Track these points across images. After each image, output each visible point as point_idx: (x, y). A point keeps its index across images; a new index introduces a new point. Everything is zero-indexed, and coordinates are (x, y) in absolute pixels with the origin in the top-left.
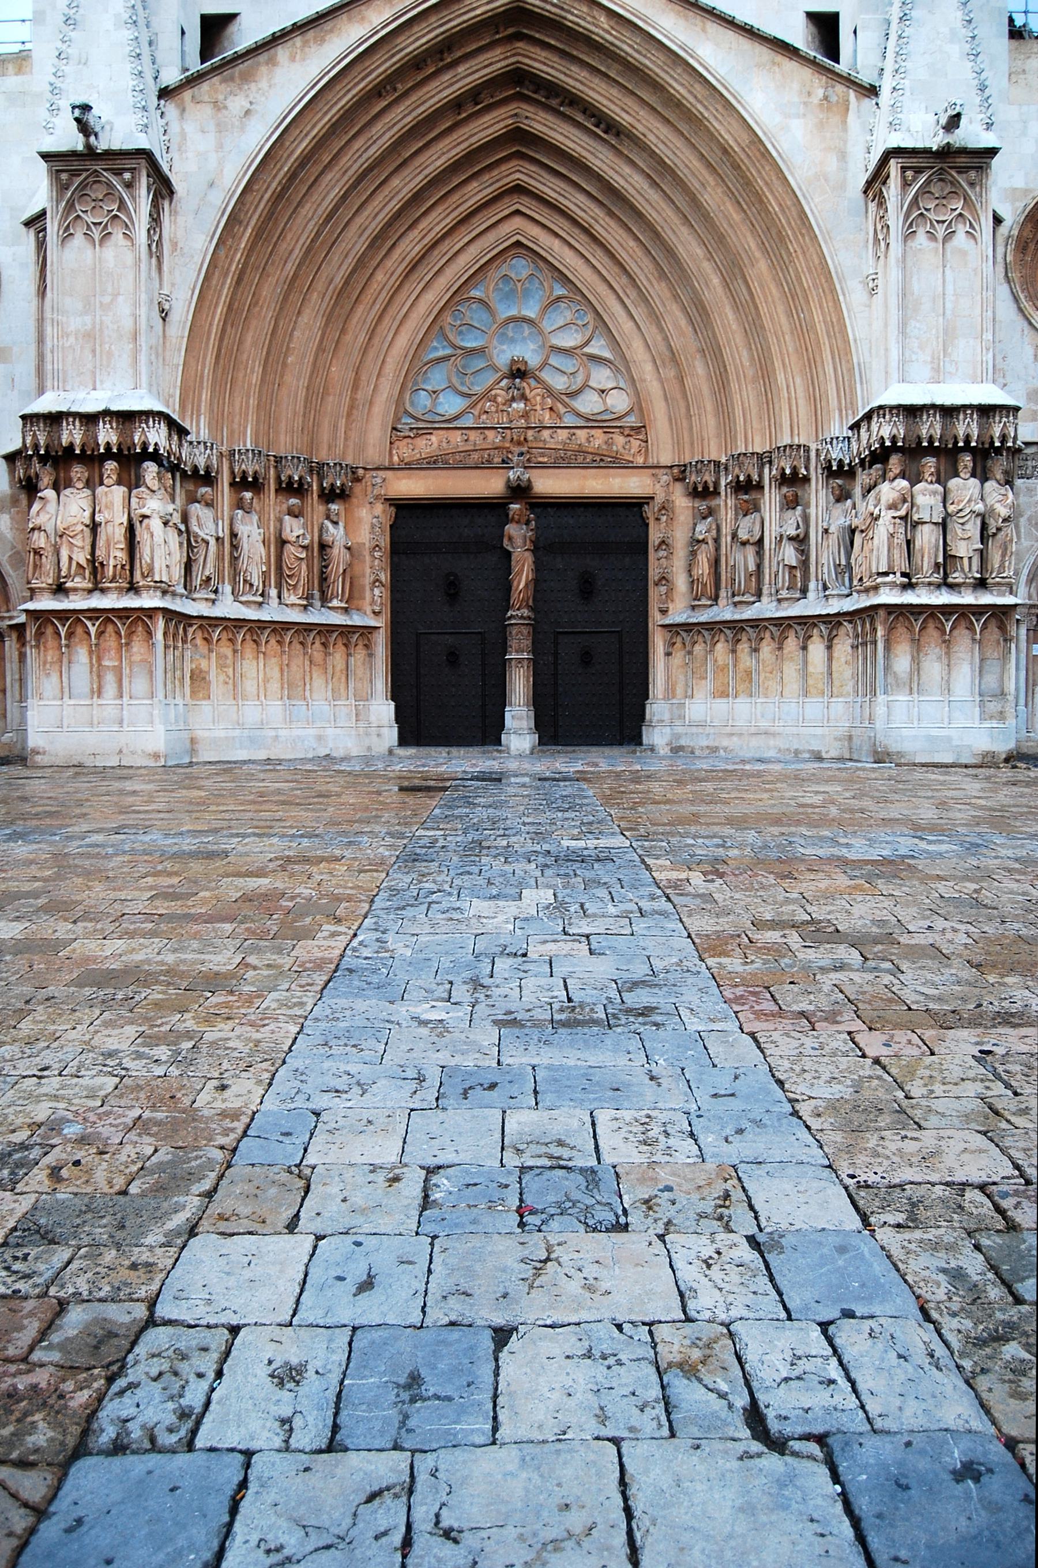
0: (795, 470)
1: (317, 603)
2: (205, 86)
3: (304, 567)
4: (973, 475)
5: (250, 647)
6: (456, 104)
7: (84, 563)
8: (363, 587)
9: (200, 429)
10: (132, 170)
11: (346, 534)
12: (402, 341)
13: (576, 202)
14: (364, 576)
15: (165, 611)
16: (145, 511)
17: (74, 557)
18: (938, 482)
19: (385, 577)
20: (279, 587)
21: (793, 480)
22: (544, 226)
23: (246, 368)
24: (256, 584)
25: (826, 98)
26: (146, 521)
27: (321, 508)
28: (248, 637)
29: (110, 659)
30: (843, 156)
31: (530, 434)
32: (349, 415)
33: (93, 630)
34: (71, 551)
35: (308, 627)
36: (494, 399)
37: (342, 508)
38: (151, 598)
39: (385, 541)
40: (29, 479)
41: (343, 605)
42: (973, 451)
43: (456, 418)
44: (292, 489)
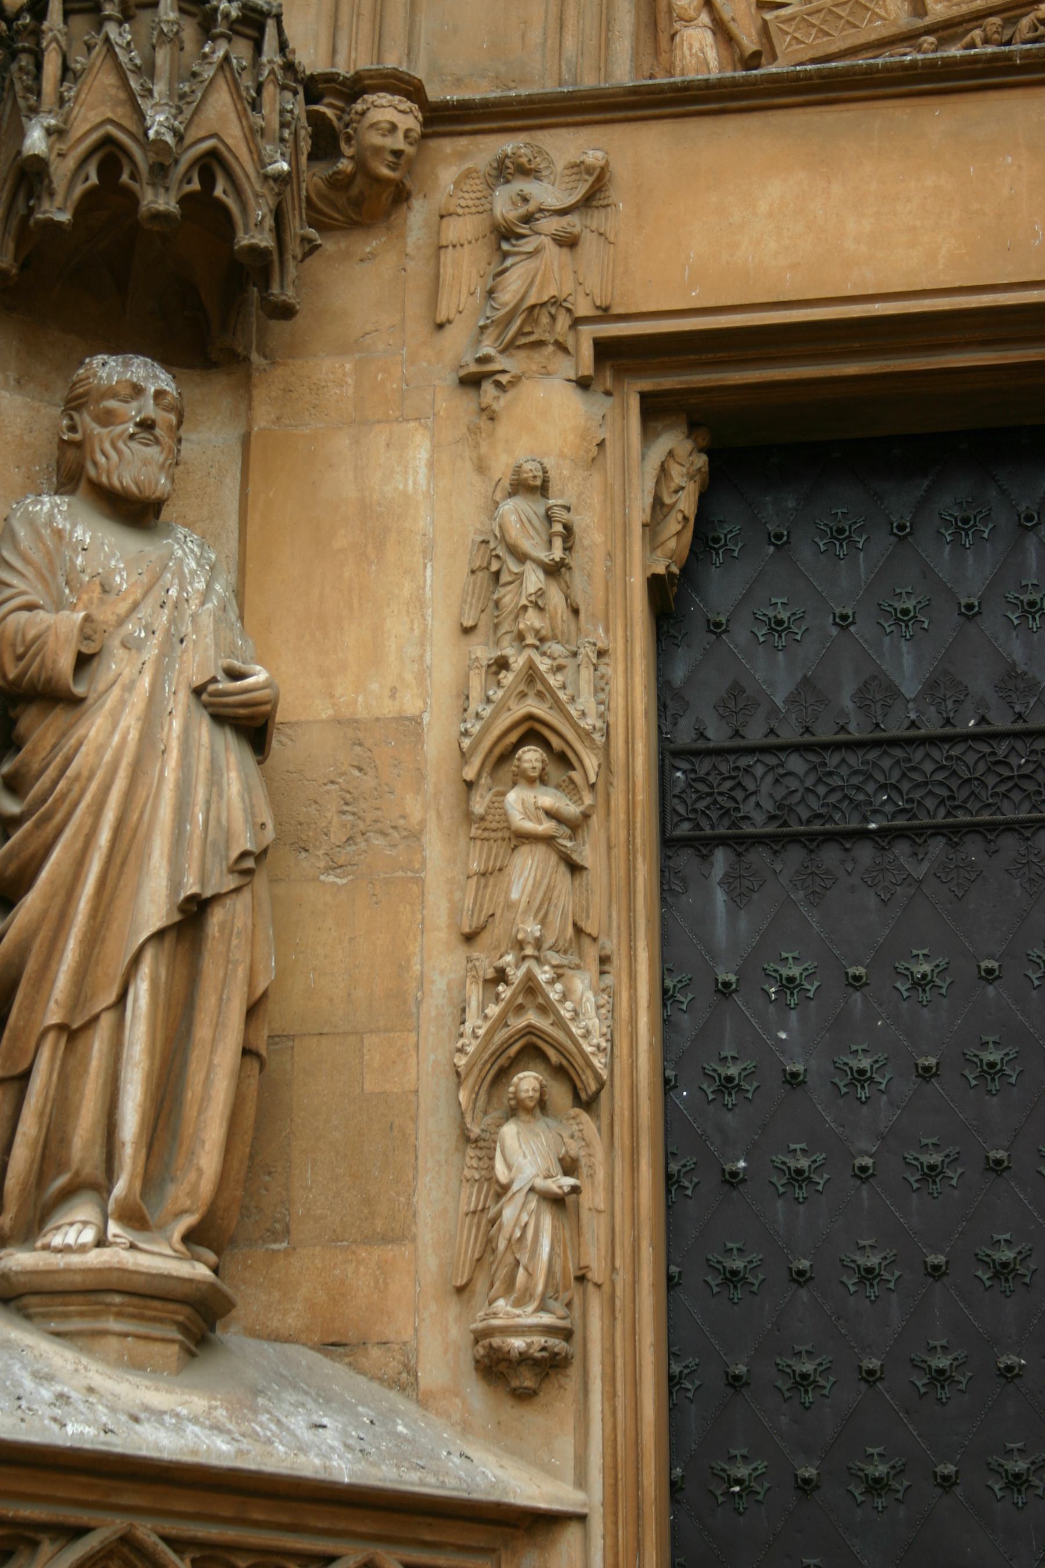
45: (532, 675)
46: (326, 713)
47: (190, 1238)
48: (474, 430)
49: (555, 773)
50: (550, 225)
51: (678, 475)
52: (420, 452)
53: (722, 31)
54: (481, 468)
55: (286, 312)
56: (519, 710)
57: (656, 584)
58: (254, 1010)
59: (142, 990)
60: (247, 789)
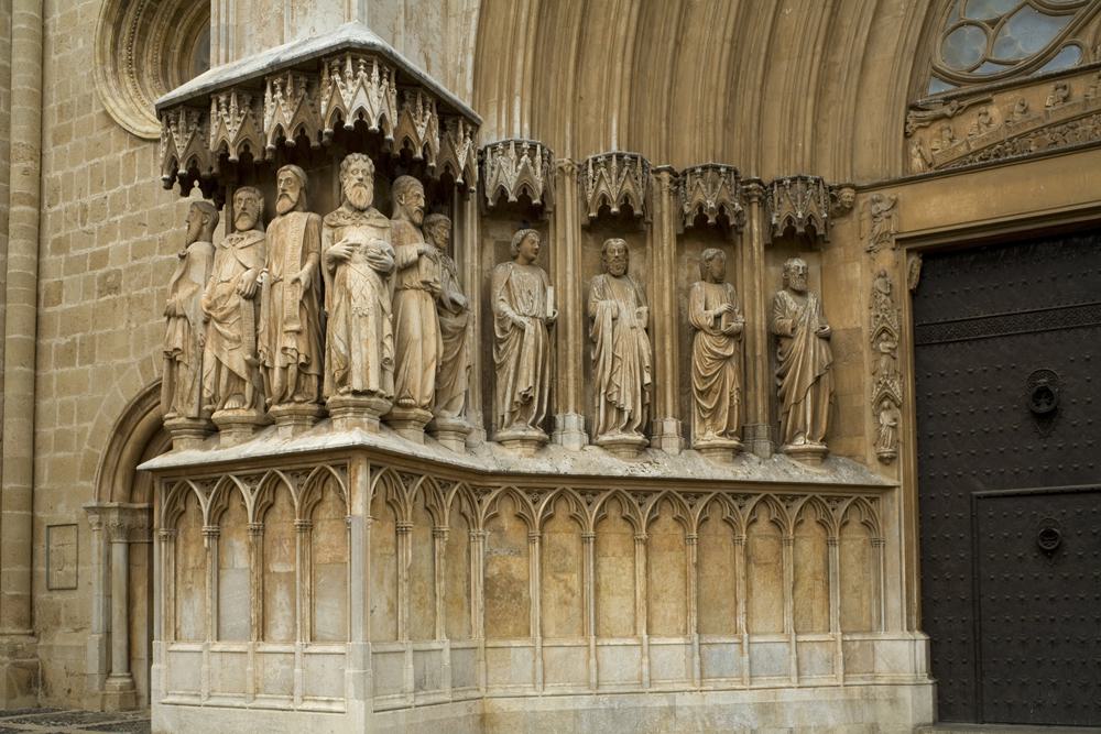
1: (765, 446)
3: (731, 373)
5: (615, 533)
7: (241, 371)
8: (859, 413)
9: (507, 122)
11: (822, 313)
14: (860, 389)
15: (377, 459)
16: (339, 249)
17: (224, 360)
19: (902, 388)
20: (684, 415)
23: (607, 14)
24: (628, 407)
26: (340, 270)
27: (775, 271)
28: (613, 512)
29: (283, 560)
32: (820, 95)
33: (250, 501)
34: (220, 349)
35: (741, 491)
37: (814, 269)
38: (350, 428)
39: (902, 319)
41: (817, 446)
43: (1044, 58)
44: (710, 230)
45: (884, 318)
46: (841, 327)
47: (821, 441)
48: (869, 262)
49: (890, 338)
50: (883, 214)
51: (915, 266)
52: (858, 269)
53: (922, 157)
54: (872, 271)
55: (829, 242)
56: (881, 326)
57: (911, 291)
58: (830, 396)
59: (809, 395)
60: (827, 352)
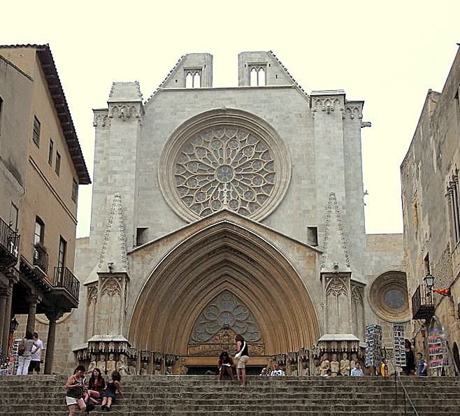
0: (305, 357)
2: (139, 252)
4: (348, 359)
6: (209, 254)
9: (134, 346)
10: (122, 278)
12: (191, 319)
13: (242, 279)
18: (337, 361)
21: (305, 360)
22: (234, 285)
25: (310, 255)
30: (315, 271)
31: (230, 346)
36: (219, 335)
40: (82, 358)
42: (347, 352)
43: (208, 341)
44: (158, 362)
